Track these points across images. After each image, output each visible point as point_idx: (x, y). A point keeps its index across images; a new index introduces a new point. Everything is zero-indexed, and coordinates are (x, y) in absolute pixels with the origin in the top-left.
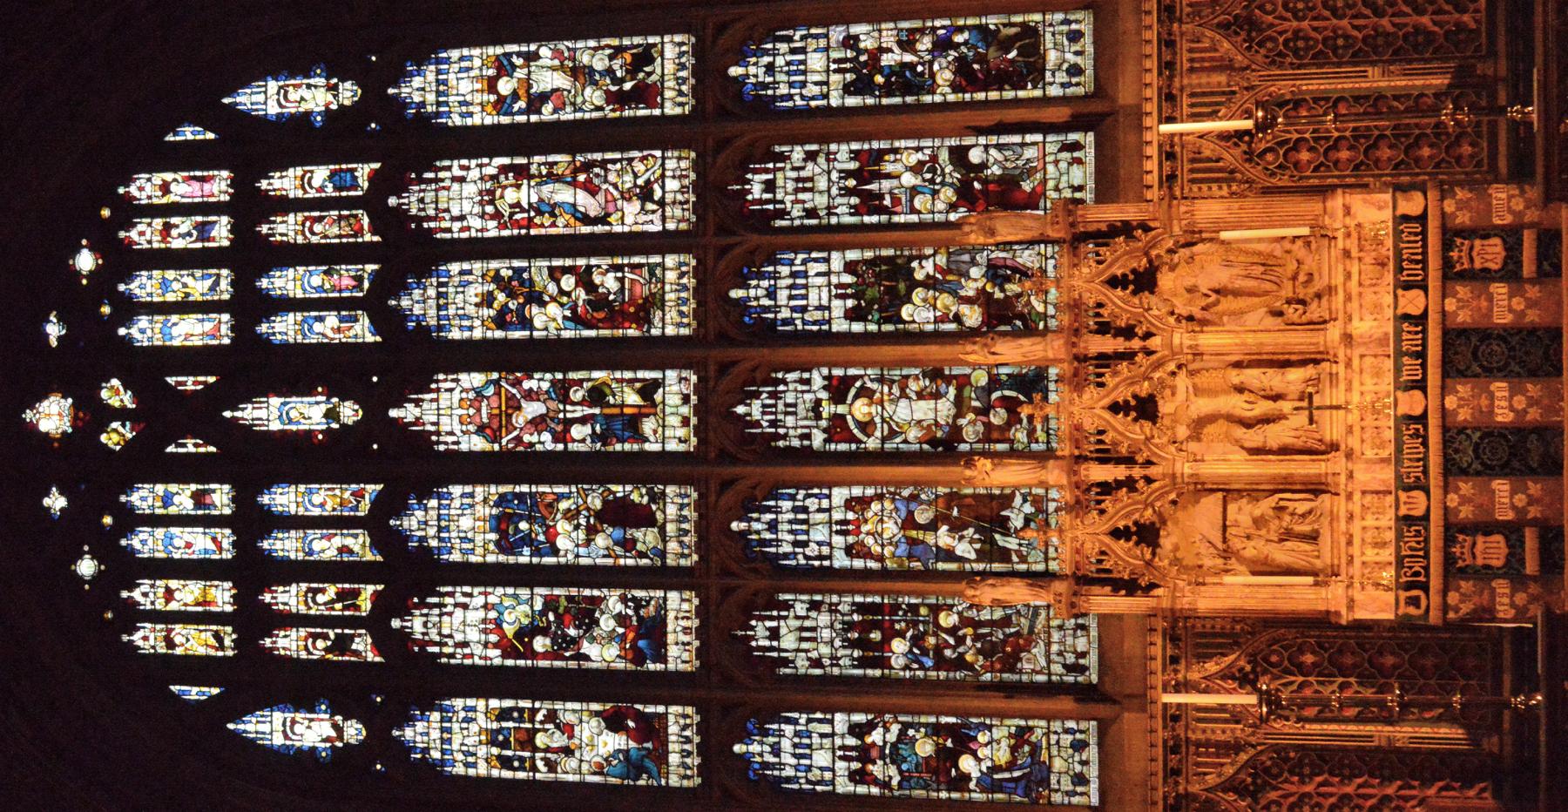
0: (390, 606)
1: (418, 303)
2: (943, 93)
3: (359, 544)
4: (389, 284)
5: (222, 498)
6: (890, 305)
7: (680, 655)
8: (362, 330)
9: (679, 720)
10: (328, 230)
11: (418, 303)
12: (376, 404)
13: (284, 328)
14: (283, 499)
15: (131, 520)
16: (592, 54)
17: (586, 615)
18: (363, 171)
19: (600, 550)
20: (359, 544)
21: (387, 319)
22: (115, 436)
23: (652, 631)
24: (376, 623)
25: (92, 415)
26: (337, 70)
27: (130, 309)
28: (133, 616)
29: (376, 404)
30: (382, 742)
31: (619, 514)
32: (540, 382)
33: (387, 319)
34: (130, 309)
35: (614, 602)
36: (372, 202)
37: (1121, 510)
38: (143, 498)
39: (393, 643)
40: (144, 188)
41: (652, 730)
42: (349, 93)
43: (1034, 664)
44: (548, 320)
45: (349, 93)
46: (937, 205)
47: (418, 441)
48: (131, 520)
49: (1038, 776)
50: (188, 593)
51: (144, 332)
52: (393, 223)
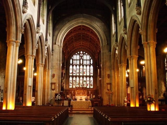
0: (75, 65)
1: (85, 66)
2: (91, 83)
3: (77, 64)
4: (85, 65)
5: (79, 59)
6: (84, 81)
7: (74, 75)
8: (84, 64)
9: (72, 75)
10: (87, 63)
11: (85, 66)
12: (82, 64)
13: (84, 61)
14: (79, 61)
15: (78, 55)
16: (92, 72)
17: (75, 71)
18: (89, 64)
19: (77, 72)
20: (77, 64)
21: (84, 65)
22: (81, 55)
23: (74, 74)
24: (75, 64)
25: (81, 54)
26: (92, 63)
27: (85, 55)
28: (75, 55)
29: (82, 64)
30: (71, 64)
31: (78, 73)
32: (82, 70)
33: (84, 65)
34: (85, 55)
35: (75, 72)
36: (88, 64)
37: (78, 89)
38: (79, 56)
39: (74, 65)
40: (89, 56)
41: (71, 74)
42: (92, 64)
43: (73, 86)
44: (84, 71)
45: (92, 64)
46: (87, 83)
47: (80, 66)
48: (78, 55)
49: (70, 86)
50: (76, 57)
51: (84, 56)
52: (87, 65)
